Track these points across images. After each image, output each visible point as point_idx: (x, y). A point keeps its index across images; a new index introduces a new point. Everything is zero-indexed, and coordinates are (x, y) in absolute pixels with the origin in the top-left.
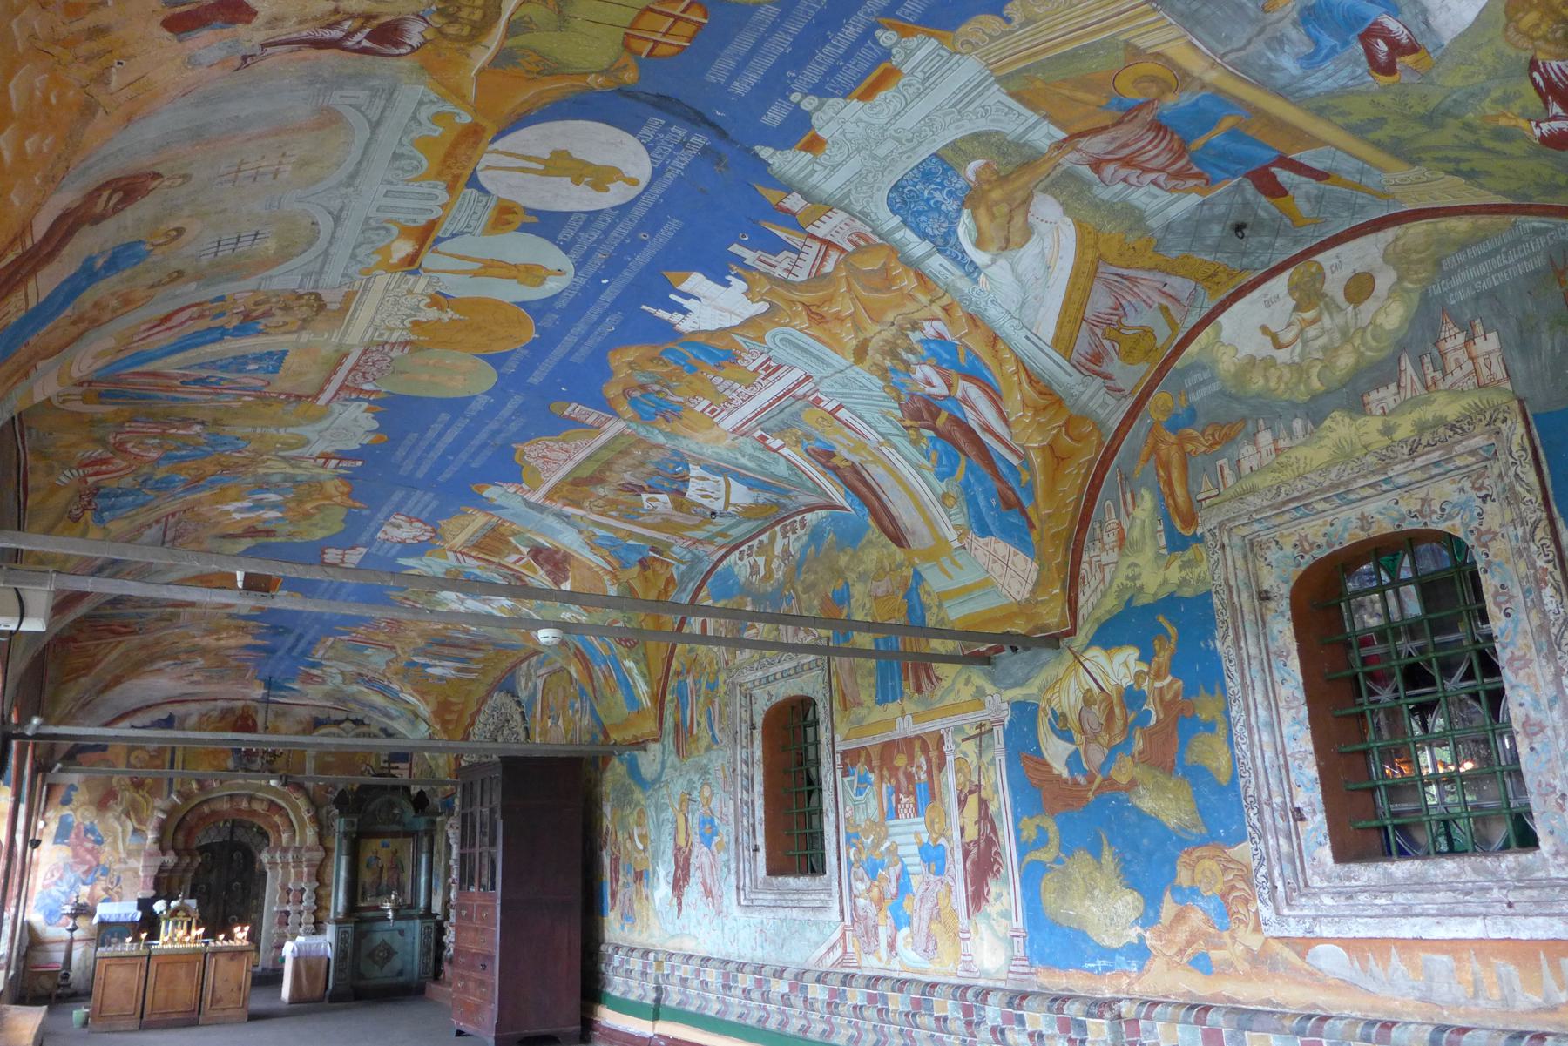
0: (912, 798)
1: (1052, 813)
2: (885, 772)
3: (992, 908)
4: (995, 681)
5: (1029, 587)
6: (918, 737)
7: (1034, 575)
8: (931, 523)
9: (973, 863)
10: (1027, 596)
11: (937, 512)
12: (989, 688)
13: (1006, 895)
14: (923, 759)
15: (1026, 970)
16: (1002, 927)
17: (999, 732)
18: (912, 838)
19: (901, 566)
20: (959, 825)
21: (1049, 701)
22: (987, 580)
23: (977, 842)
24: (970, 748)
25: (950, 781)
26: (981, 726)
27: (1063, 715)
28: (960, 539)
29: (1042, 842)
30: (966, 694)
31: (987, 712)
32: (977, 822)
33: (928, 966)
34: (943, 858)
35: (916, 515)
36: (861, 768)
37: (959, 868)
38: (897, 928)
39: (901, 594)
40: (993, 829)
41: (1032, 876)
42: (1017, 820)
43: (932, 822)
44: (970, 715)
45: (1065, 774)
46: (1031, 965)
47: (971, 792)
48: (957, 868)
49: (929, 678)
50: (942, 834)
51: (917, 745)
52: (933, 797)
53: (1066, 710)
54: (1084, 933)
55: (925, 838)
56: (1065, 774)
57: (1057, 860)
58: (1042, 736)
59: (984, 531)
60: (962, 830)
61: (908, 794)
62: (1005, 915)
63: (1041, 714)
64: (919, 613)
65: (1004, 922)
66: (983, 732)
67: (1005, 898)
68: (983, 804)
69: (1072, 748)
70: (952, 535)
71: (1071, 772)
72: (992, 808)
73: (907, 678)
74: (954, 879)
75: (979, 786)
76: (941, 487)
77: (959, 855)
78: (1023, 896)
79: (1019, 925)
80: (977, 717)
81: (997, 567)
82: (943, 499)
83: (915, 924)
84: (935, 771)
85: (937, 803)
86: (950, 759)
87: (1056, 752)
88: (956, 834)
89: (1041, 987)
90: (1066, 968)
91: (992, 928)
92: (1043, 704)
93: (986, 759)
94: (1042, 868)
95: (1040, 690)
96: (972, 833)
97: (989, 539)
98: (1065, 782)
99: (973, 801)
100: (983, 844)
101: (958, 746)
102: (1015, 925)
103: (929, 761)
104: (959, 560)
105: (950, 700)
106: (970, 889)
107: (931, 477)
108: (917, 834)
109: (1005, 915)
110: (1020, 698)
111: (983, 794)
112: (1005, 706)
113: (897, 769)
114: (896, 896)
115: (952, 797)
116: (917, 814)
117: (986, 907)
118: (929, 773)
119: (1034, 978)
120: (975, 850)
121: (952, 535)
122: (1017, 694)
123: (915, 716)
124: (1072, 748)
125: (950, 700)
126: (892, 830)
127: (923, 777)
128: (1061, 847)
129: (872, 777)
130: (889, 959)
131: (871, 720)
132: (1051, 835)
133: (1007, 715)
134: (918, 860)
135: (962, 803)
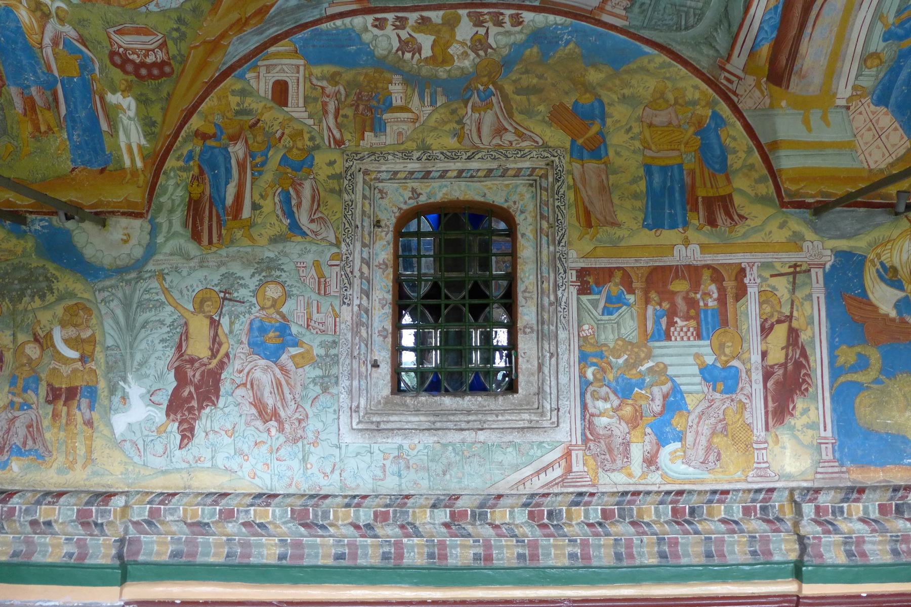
0: (693, 323)
1: (876, 344)
2: (653, 295)
3: (798, 421)
4: (816, 230)
5: (890, 160)
6: (708, 267)
7: (902, 151)
8: (831, 73)
9: (777, 383)
10: (883, 166)
11: (850, 68)
12: (809, 234)
13: (815, 411)
14: (713, 288)
15: (836, 470)
16: (808, 437)
17: (817, 275)
18: (691, 360)
19: (694, 103)
20: (756, 352)
21: (879, 256)
22: (849, 143)
23: (784, 365)
24: (782, 286)
25: (751, 311)
26: (795, 266)
27: (894, 269)
28: (849, 99)
29: (862, 364)
30: (780, 236)
31: (802, 255)
32: (786, 348)
33: (707, 476)
34: (736, 378)
35: (824, 61)
36: (614, 287)
37: (758, 387)
38: (662, 441)
39: (692, 130)
40: (804, 354)
41: (844, 397)
42: (832, 348)
43: (722, 346)
44: (784, 255)
45: (893, 314)
46: (842, 465)
47: (779, 322)
48: (755, 390)
49: (729, 215)
50: (737, 357)
51: (706, 275)
52: (725, 323)
53: (896, 263)
54: (904, 437)
55: (710, 360)
56: (893, 314)
57: (876, 381)
58: (868, 282)
59: (882, 100)
60: (764, 355)
61: (687, 318)
62: (813, 426)
63: (868, 264)
64: (718, 152)
65: (810, 432)
66: (796, 272)
67: (812, 414)
68: (793, 335)
69: (901, 294)
70: (844, 92)
71: (899, 312)
72: (804, 337)
73: (697, 210)
74: (749, 397)
75: (790, 318)
76: (877, 44)
77: (757, 376)
78: (834, 410)
79: (829, 433)
80: (794, 257)
81: (868, 136)
82: (867, 58)
83: (690, 438)
84: (730, 300)
85: (731, 329)
86: (752, 291)
87: (884, 298)
88: (756, 358)
89: (854, 481)
90: (883, 465)
91: (796, 437)
92: (872, 256)
93: (800, 294)
94: (860, 387)
95: (870, 245)
96: (777, 356)
97: (882, 109)
98: (893, 320)
99: (781, 331)
100: (790, 366)
101: (764, 280)
102: (823, 434)
103: (722, 290)
104: (831, 117)
105: (758, 238)
106: (771, 405)
107: (879, 29)
108: (697, 356)
109: (813, 426)
110: (845, 248)
111: (795, 324)
112: (829, 252)
113: (674, 293)
114: (661, 414)
115: (753, 323)
116: (699, 336)
117: (790, 421)
118: (722, 300)
119: (847, 476)
120: (781, 372)
121: (844, 92)
122: (843, 244)
123: (703, 247)
124: (901, 294)
125: (758, 238)
126: (657, 352)
127: (712, 303)
128: (882, 371)
129: (631, 298)
130: (644, 475)
131: (635, 241)
132: (873, 361)
133: (829, 261)
134: (698, 379)
135: (766, 330)
